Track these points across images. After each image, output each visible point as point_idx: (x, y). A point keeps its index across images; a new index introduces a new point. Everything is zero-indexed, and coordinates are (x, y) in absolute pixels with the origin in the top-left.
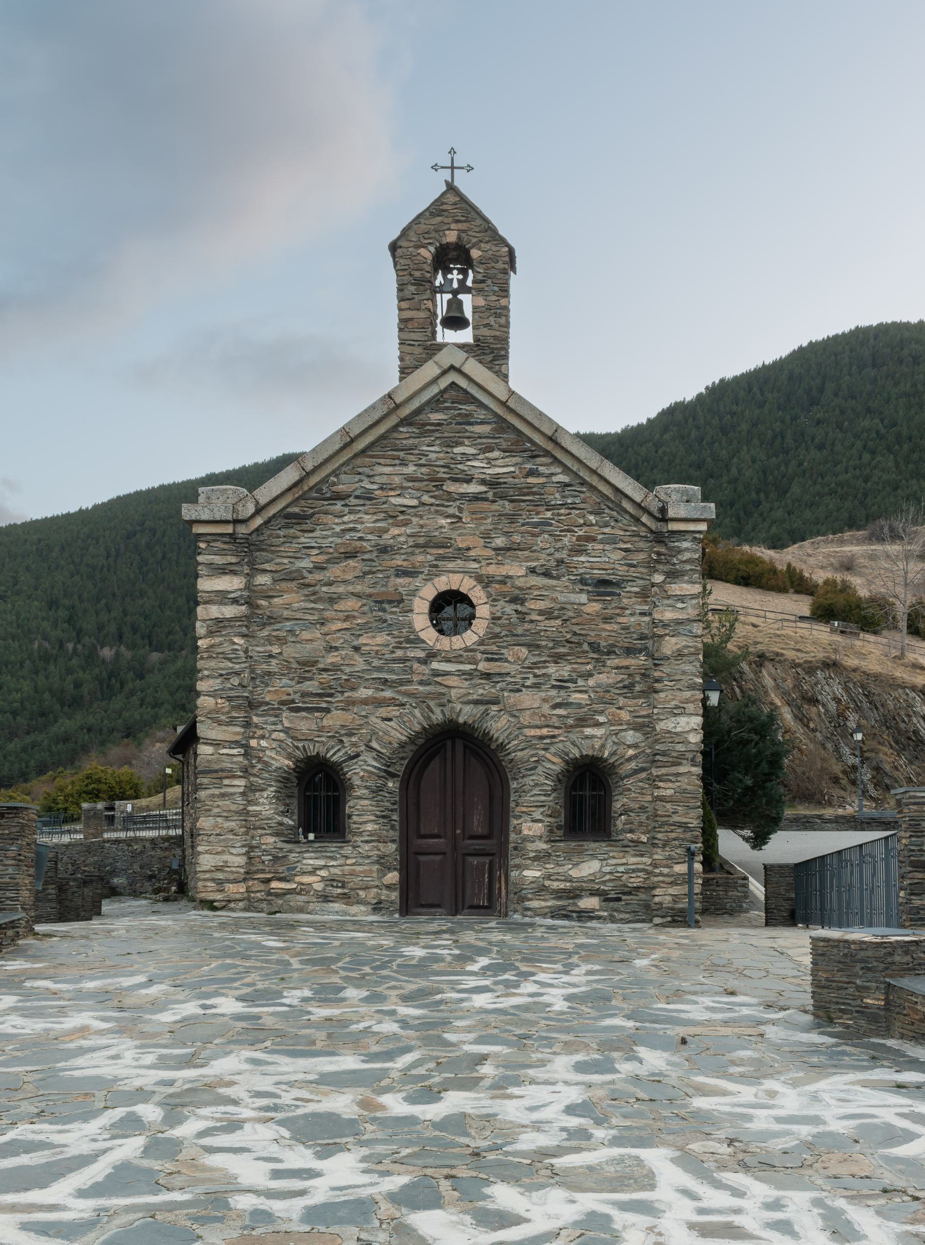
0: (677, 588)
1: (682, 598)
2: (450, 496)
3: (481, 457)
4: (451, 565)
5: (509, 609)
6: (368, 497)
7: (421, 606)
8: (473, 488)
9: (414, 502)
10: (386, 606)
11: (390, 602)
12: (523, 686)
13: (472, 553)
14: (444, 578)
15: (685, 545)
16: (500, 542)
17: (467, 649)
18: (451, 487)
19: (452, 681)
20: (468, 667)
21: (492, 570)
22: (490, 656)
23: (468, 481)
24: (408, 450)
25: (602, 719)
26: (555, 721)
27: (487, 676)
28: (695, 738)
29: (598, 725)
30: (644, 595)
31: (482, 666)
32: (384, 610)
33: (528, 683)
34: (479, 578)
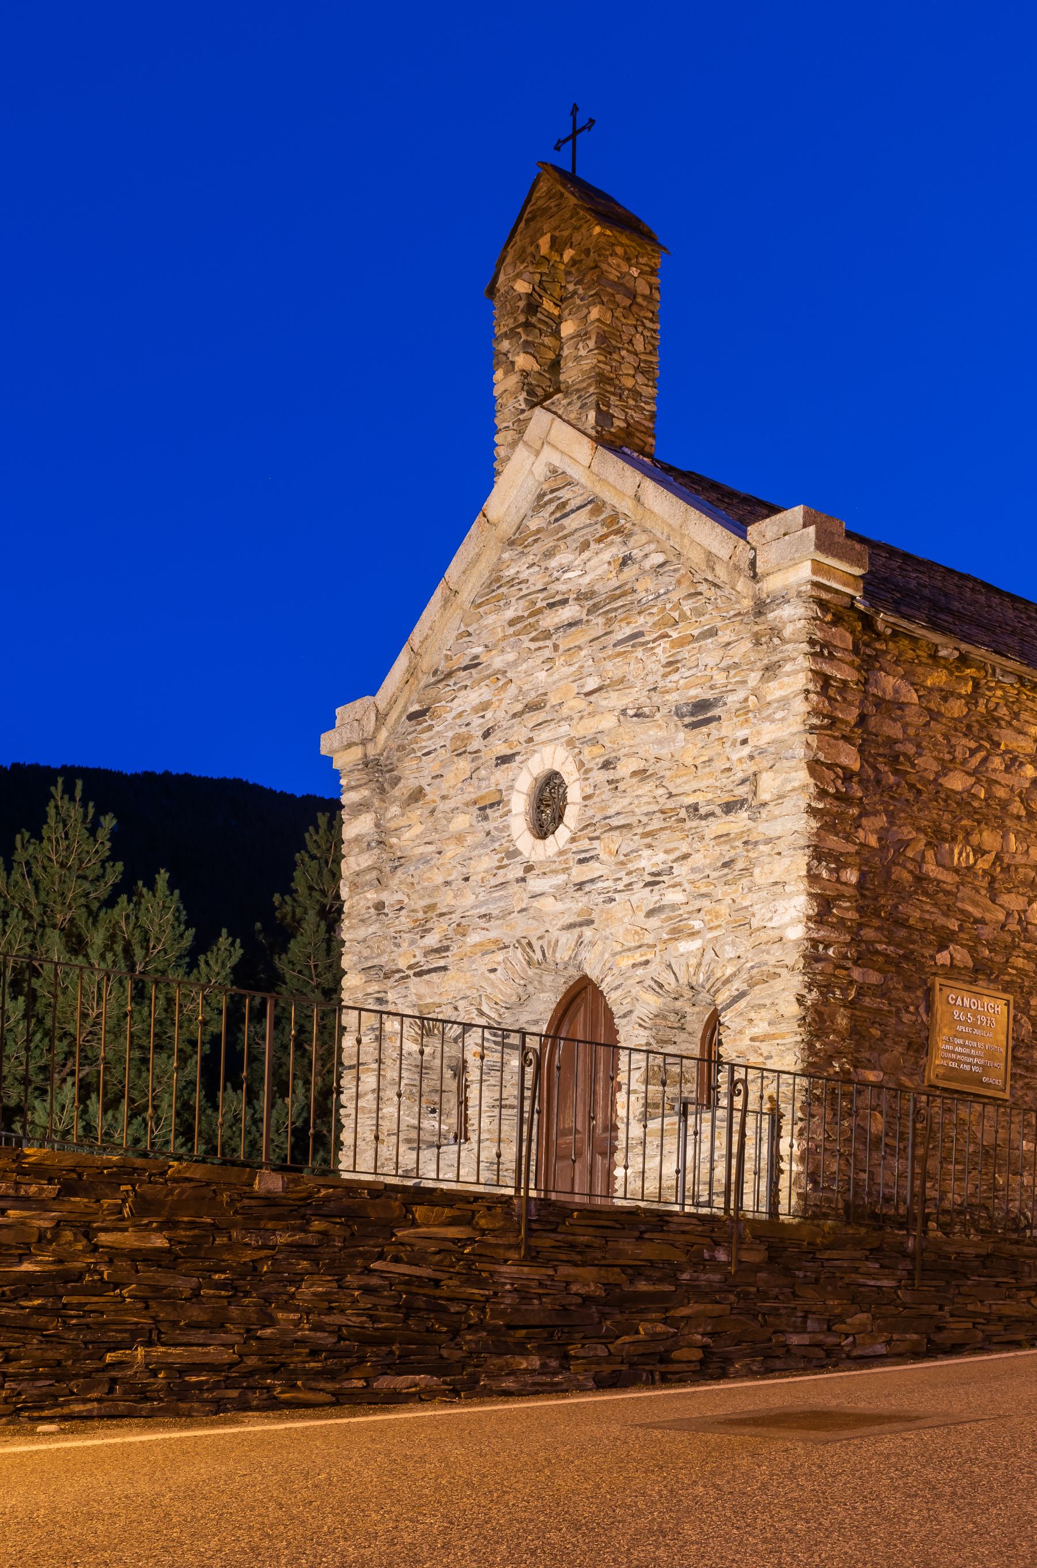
0: (775, 690)
1: (784, 702)
2: (547, 635)
3: (576, 563)
4: (544, 735)
5: (601, 776)
6: (474, 664)
7: (520, 803)
8: (567, 613)
9: (511, 657)
10: (488, 811)
11: (492, 805)
12: (616, 891)
13: (565, 711)
14: (537, 757)
15: (786, 612)
16: (592, 683)
17: (561, 853)
18: (550, 620)
19: (548, 904)
20: (561, 878)
21: (587, 727)
22: (582, 856)
23: (564, 602)
24: (511, 582)
25: (697, 925)
26: (649, 939)
27: (580, 886)
28: (797, 932)
29: (694, 934)
30: (743, 710)
31: (580, 873)
32: (486, 818)
33: (620, 886)
34: (570, 743)
